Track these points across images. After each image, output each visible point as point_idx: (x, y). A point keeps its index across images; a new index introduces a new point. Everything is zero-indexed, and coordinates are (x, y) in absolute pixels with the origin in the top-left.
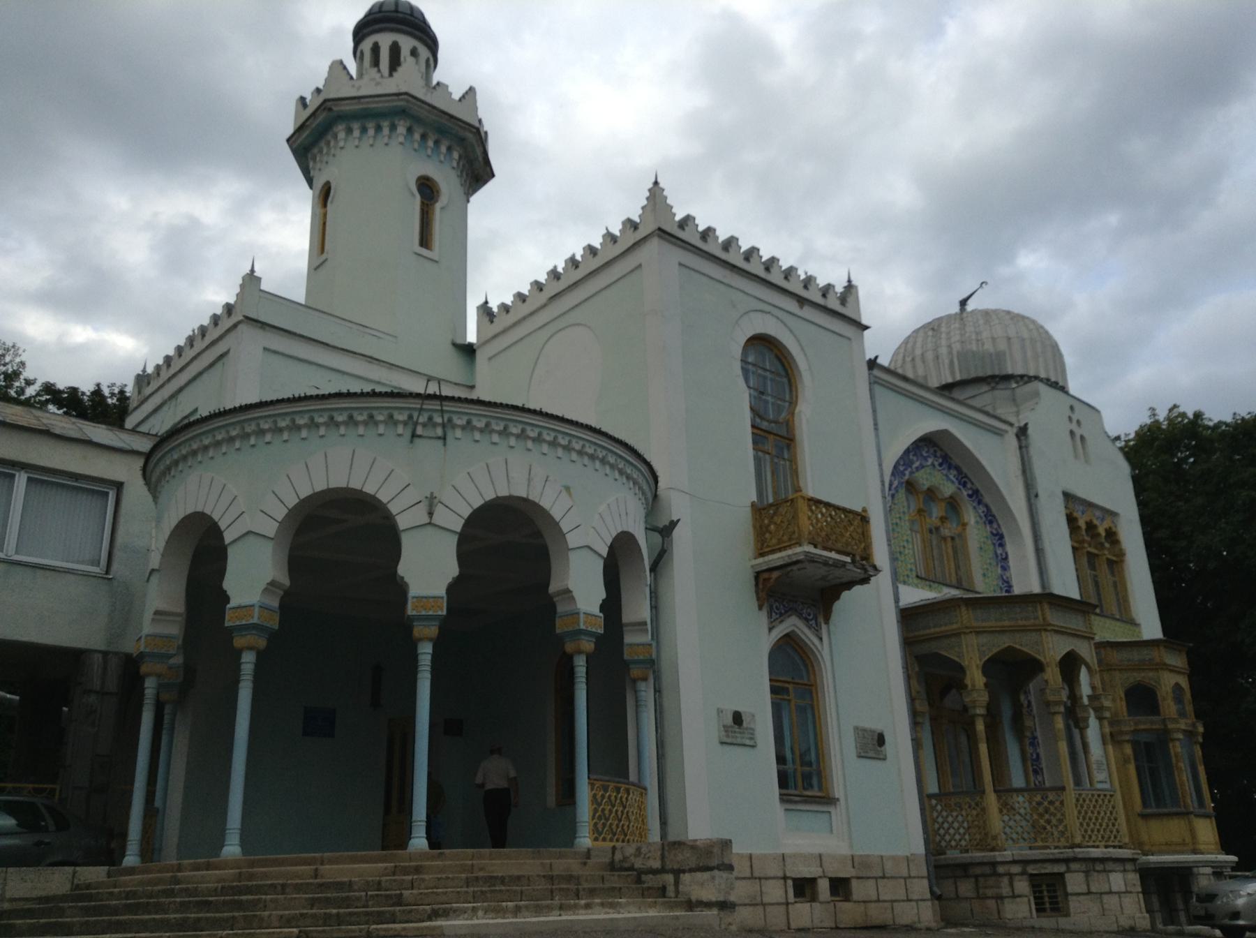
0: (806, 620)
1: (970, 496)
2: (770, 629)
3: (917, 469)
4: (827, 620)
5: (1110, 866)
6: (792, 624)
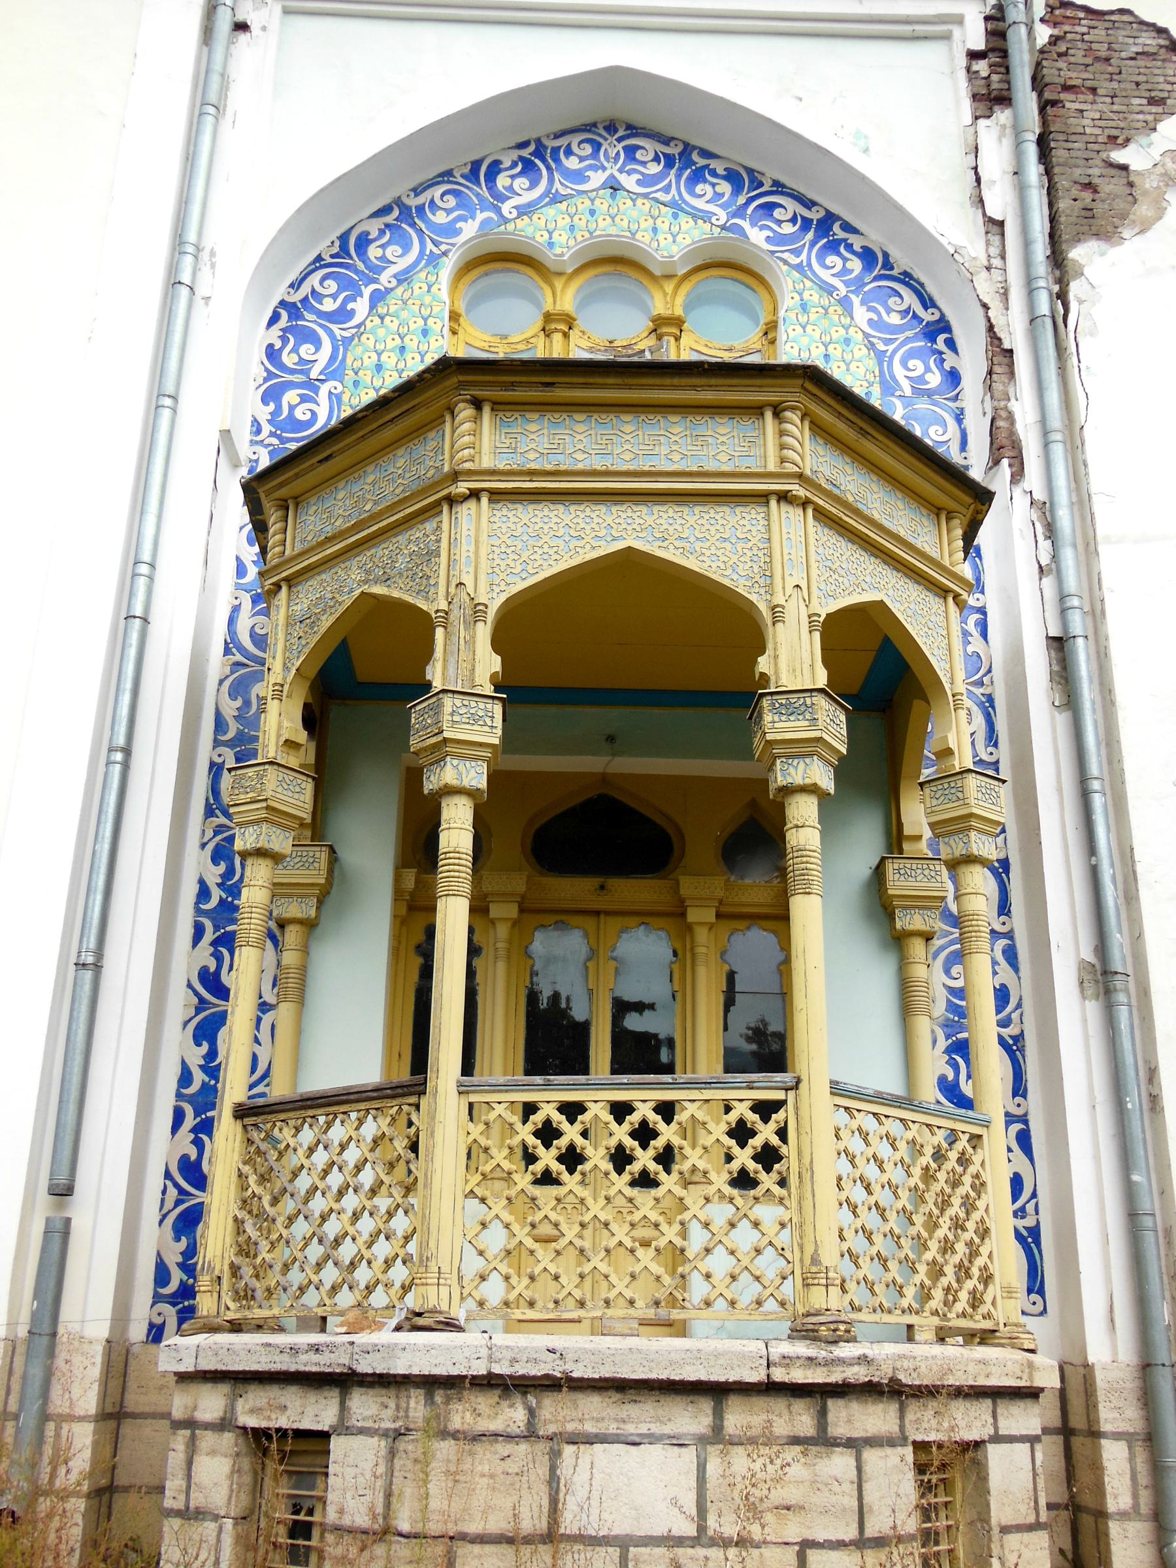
3: (524, 211)
5: (556, 1412)
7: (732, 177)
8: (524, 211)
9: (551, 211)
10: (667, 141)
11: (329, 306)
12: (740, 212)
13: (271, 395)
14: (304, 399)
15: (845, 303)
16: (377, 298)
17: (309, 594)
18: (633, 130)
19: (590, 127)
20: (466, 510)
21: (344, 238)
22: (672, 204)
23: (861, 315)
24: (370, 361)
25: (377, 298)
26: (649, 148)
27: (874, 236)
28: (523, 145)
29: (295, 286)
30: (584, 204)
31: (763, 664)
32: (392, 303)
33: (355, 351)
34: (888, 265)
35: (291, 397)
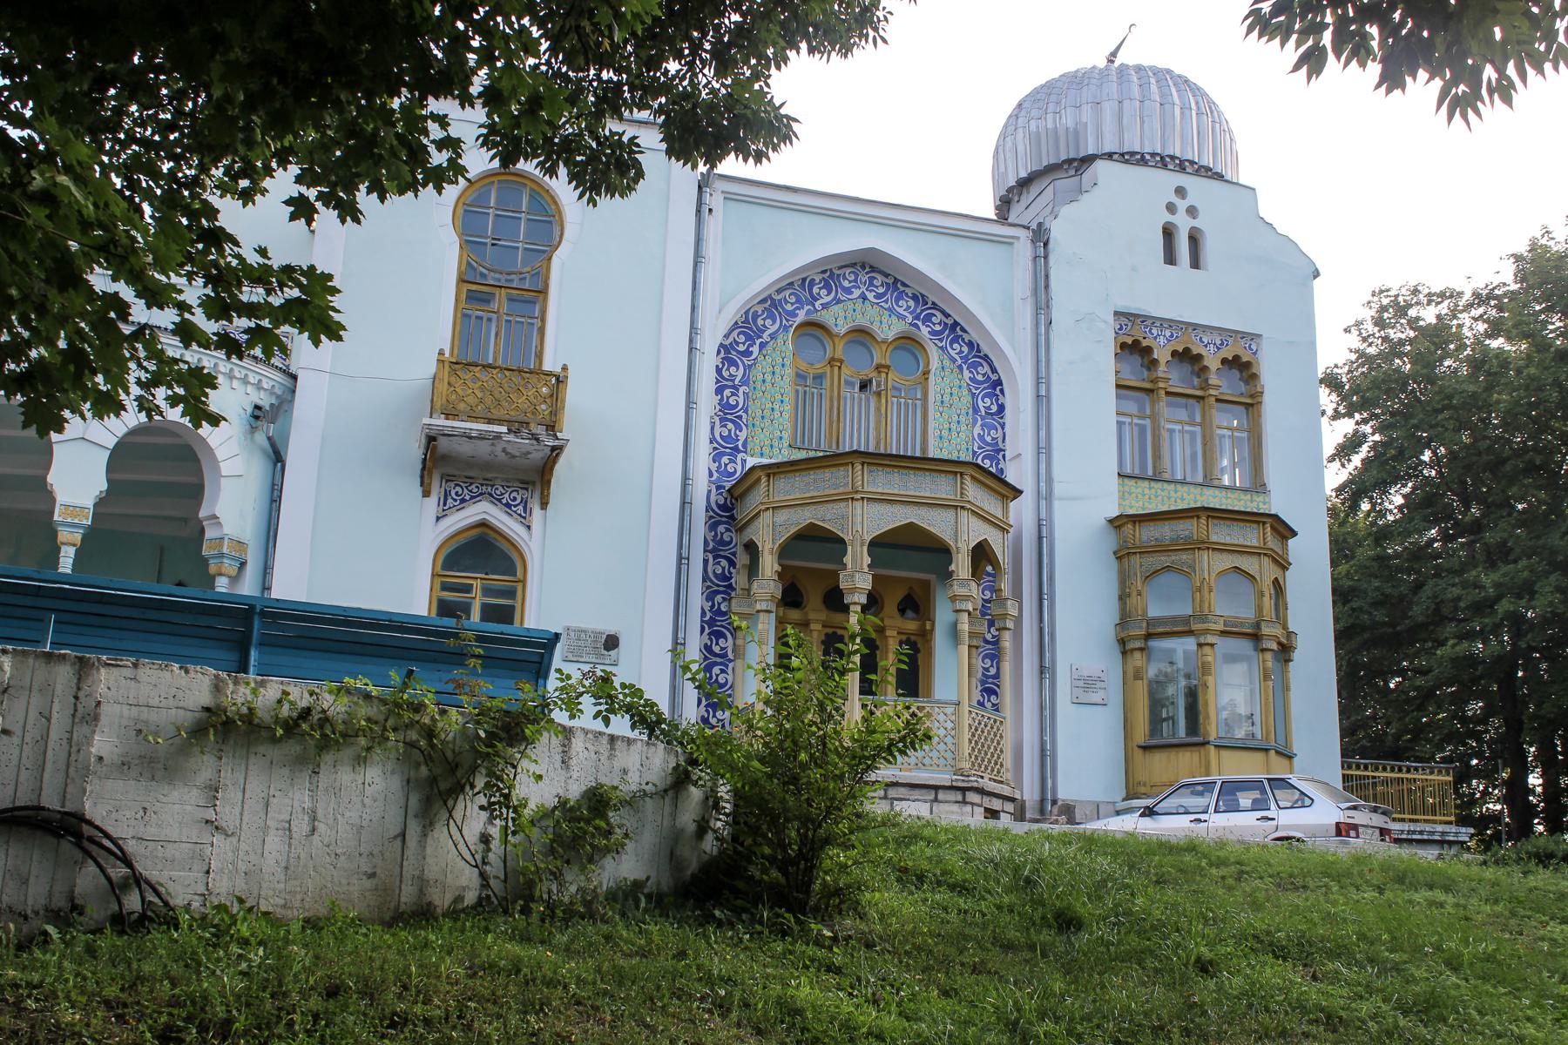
0: (508, 505)
1: (933, 333)
2: (438, 519)
4: (544, 505)
6: (481, 510)
7: (915, 298)
8: (825, 306)
9: (836, 308)
10: (887, 276)
11: (742, 348)
12: (917, 318)
13: (719, 391)
14: (733, 394)
15: (960, 368)
16: (762, 346)
17: (782, 517)
18: (873, 269)
19: (853, 265)
20: (858, 504)
21: (746, 313)
22: (889, 309)
23: (967, 374)
24: (760, 378)
25: (762, 346)
26: (879, 279)
27: (974, 336)
28: (824, 272)
29: (726, 336)
30: (850, 305)
31: (952, 567)
32: (769, 347)
33: (754, 372)
34: (979, 351)
35: (727, 392)
